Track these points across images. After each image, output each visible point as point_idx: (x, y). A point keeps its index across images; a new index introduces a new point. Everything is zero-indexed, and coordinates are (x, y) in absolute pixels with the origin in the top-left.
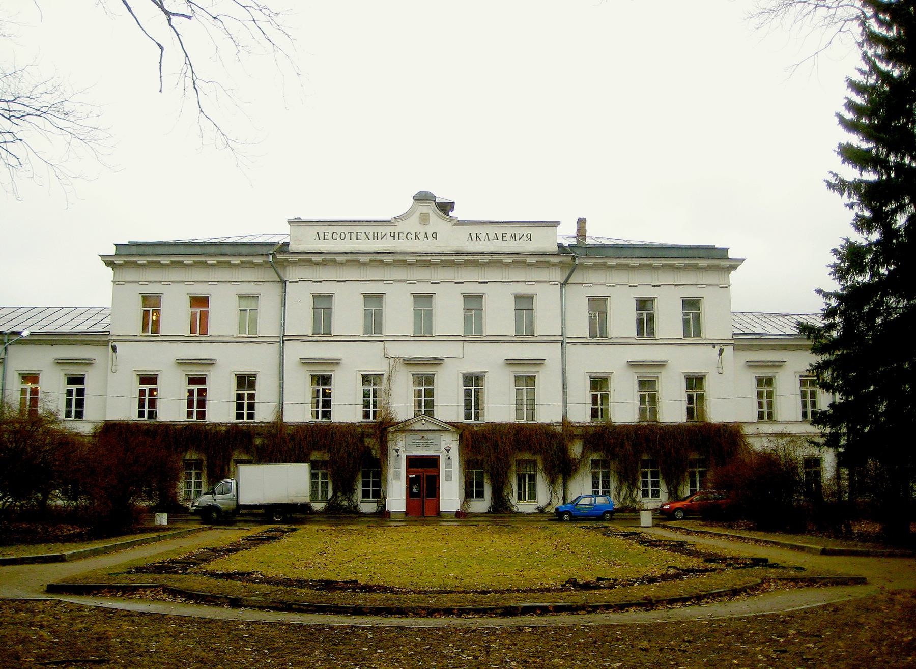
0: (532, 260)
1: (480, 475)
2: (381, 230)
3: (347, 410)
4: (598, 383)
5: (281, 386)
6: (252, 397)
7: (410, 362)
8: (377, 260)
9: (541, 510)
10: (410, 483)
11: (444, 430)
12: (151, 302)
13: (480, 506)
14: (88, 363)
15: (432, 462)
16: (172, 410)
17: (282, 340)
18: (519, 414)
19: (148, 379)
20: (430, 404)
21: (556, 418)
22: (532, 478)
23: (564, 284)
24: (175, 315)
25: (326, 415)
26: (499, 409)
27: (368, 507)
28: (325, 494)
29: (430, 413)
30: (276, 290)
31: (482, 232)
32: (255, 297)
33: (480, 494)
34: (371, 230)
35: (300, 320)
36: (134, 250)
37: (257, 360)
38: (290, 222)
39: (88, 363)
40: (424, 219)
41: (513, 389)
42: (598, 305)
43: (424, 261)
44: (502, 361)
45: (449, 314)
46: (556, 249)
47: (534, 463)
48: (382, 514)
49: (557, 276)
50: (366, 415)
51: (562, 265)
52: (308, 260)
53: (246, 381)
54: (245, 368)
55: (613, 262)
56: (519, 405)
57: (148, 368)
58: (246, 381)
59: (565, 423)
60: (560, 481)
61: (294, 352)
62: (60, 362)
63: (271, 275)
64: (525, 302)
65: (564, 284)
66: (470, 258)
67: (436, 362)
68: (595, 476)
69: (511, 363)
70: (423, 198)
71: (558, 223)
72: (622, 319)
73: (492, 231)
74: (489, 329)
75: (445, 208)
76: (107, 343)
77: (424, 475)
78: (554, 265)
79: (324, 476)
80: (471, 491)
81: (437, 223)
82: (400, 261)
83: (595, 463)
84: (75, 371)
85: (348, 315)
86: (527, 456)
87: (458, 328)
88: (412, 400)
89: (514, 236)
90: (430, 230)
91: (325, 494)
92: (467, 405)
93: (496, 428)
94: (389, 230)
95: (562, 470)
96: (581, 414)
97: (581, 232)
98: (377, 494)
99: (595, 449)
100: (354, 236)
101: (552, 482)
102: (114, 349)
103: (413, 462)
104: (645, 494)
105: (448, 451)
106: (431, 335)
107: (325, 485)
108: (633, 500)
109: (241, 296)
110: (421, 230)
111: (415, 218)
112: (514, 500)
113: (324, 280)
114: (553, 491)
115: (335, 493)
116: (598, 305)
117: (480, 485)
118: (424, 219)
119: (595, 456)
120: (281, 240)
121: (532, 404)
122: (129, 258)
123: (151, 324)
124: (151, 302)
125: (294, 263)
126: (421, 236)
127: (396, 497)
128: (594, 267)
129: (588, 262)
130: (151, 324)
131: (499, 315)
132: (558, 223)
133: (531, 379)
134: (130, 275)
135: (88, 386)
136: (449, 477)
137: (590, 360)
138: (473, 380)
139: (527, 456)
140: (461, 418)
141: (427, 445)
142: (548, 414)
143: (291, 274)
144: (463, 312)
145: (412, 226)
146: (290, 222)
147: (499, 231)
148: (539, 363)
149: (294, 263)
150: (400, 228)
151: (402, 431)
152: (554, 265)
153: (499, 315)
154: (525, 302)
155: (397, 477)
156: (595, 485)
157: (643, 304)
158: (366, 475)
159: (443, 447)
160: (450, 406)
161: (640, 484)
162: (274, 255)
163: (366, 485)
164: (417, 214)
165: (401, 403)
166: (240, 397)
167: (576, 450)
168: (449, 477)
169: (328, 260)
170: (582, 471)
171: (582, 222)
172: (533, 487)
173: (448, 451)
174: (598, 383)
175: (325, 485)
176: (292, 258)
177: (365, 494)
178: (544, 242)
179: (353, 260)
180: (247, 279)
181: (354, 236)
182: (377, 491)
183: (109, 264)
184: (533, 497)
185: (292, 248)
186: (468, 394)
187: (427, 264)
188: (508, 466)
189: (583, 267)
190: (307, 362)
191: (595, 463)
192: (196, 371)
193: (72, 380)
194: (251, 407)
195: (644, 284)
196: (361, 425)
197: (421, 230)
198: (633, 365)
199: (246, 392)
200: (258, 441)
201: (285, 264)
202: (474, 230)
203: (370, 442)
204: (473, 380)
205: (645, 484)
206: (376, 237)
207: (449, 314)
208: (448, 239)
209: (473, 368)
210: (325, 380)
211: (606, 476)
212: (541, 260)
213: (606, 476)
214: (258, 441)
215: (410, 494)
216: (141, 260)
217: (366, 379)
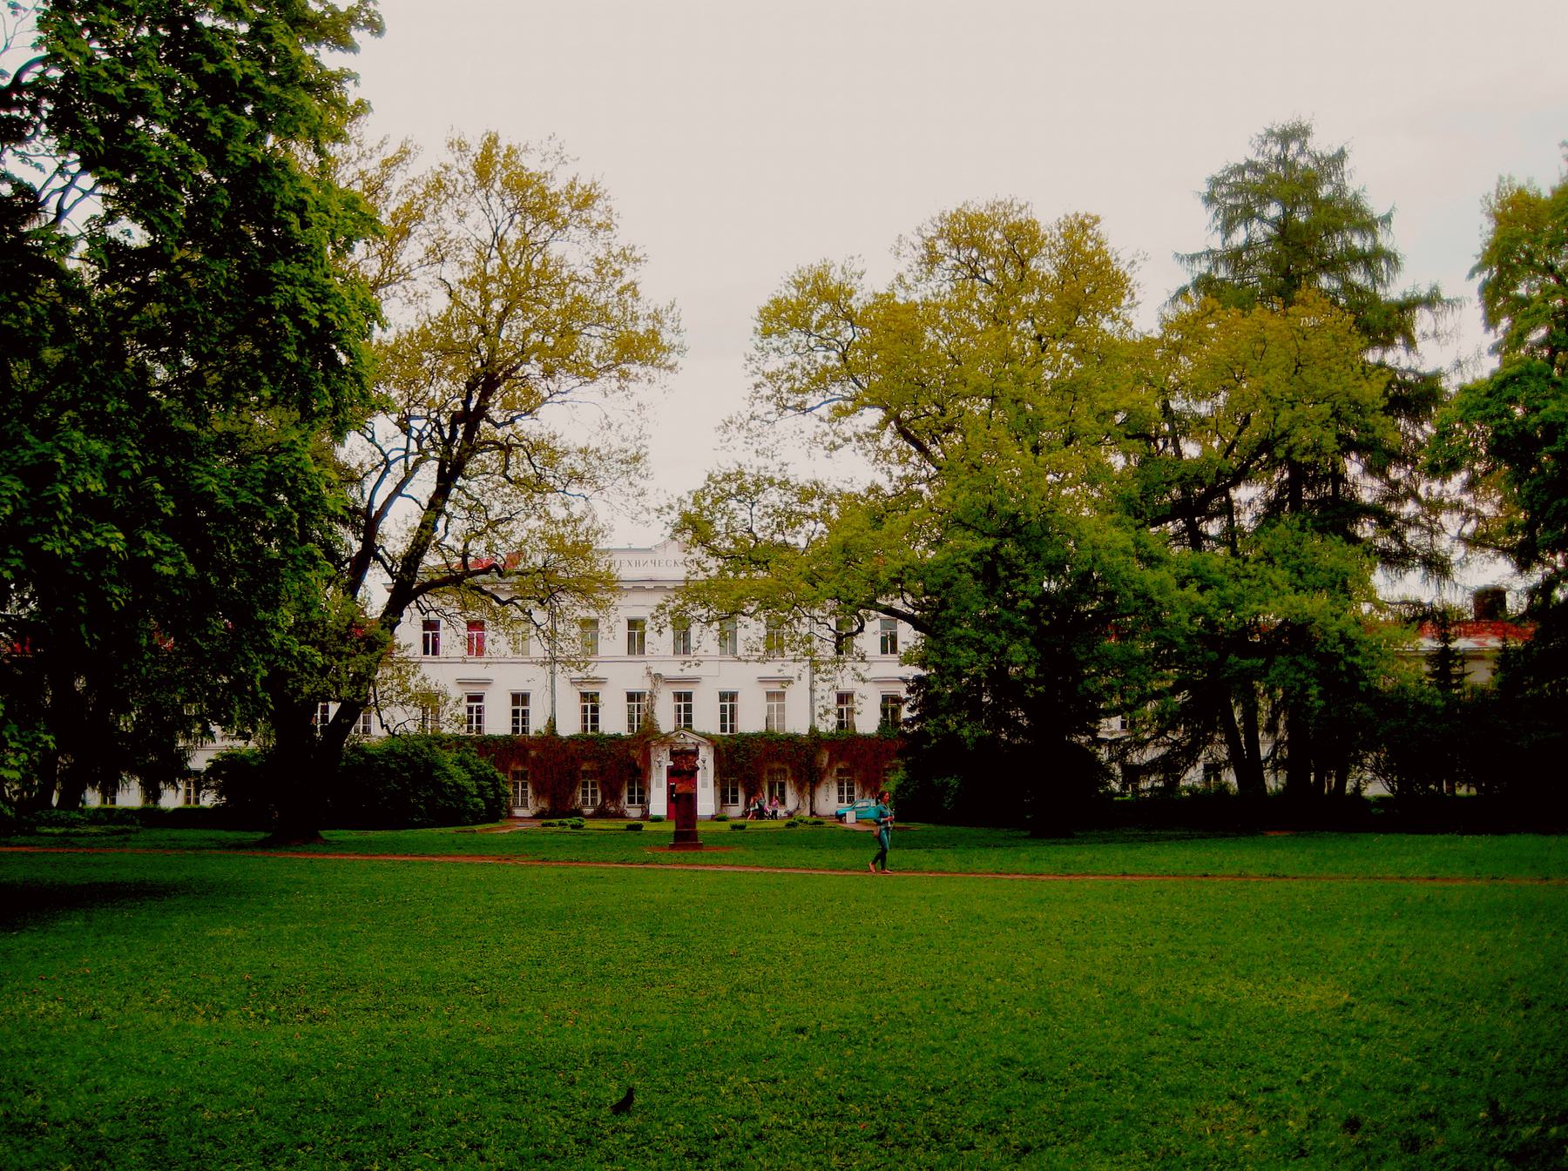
1: (735, 784)
2: (643, 557)
3: (614, 721)
5: (553, 703)
6: (525, 713)
10: (671, 790)
13: (736, 810)
20: (688, 719)
21: (804, 730)
22: (782, 786)
27: (634, 812)
29: (689, 727)
33: (735, 800)
47: (784, 771)
53: (520, 699)
54: (520, 688)
58: (520, 699)
60: (807, 789)
68: (840, 784)
79: (593, 785)
80: (725, 798)
83: (840, 772)
86: (776, 766)
88: (672, 713)
92: (723, 719)
93: (748, 738)
94: (649, 557)
95: (809, 779)
96: (827, 726)
98: (641, 800)
99: (841, 758)
101: (800, 790)
107: (594, 793)
117: (735, 792)
119: (841, 766)
135: (485, 703)
136: (705, 785)
142: (797, 723)
150: (660, 555)
156: (841, 791)
158: (631, 783)
160: (707, 720)
163: (631, 792)
165: (666, 720)
166: (515, 713)
167: (825, 758)
168: (705, 785)
170: (828, 779)
172: (782, 793)
175: (594, 793)
177: (631, 801)
184: (783, 802)
186: (723, 709)
188: (760, 775)
192: (475, 690)
199: (521, 708)
200: (533, 753)
203: (634, 753)
204: (728, 697)
206: (637, 564)
209: (728, 688)
211: (851, 784)
213: (851, 784)
214: (533, 753)
215: (671, 800)
217: (631, 697)
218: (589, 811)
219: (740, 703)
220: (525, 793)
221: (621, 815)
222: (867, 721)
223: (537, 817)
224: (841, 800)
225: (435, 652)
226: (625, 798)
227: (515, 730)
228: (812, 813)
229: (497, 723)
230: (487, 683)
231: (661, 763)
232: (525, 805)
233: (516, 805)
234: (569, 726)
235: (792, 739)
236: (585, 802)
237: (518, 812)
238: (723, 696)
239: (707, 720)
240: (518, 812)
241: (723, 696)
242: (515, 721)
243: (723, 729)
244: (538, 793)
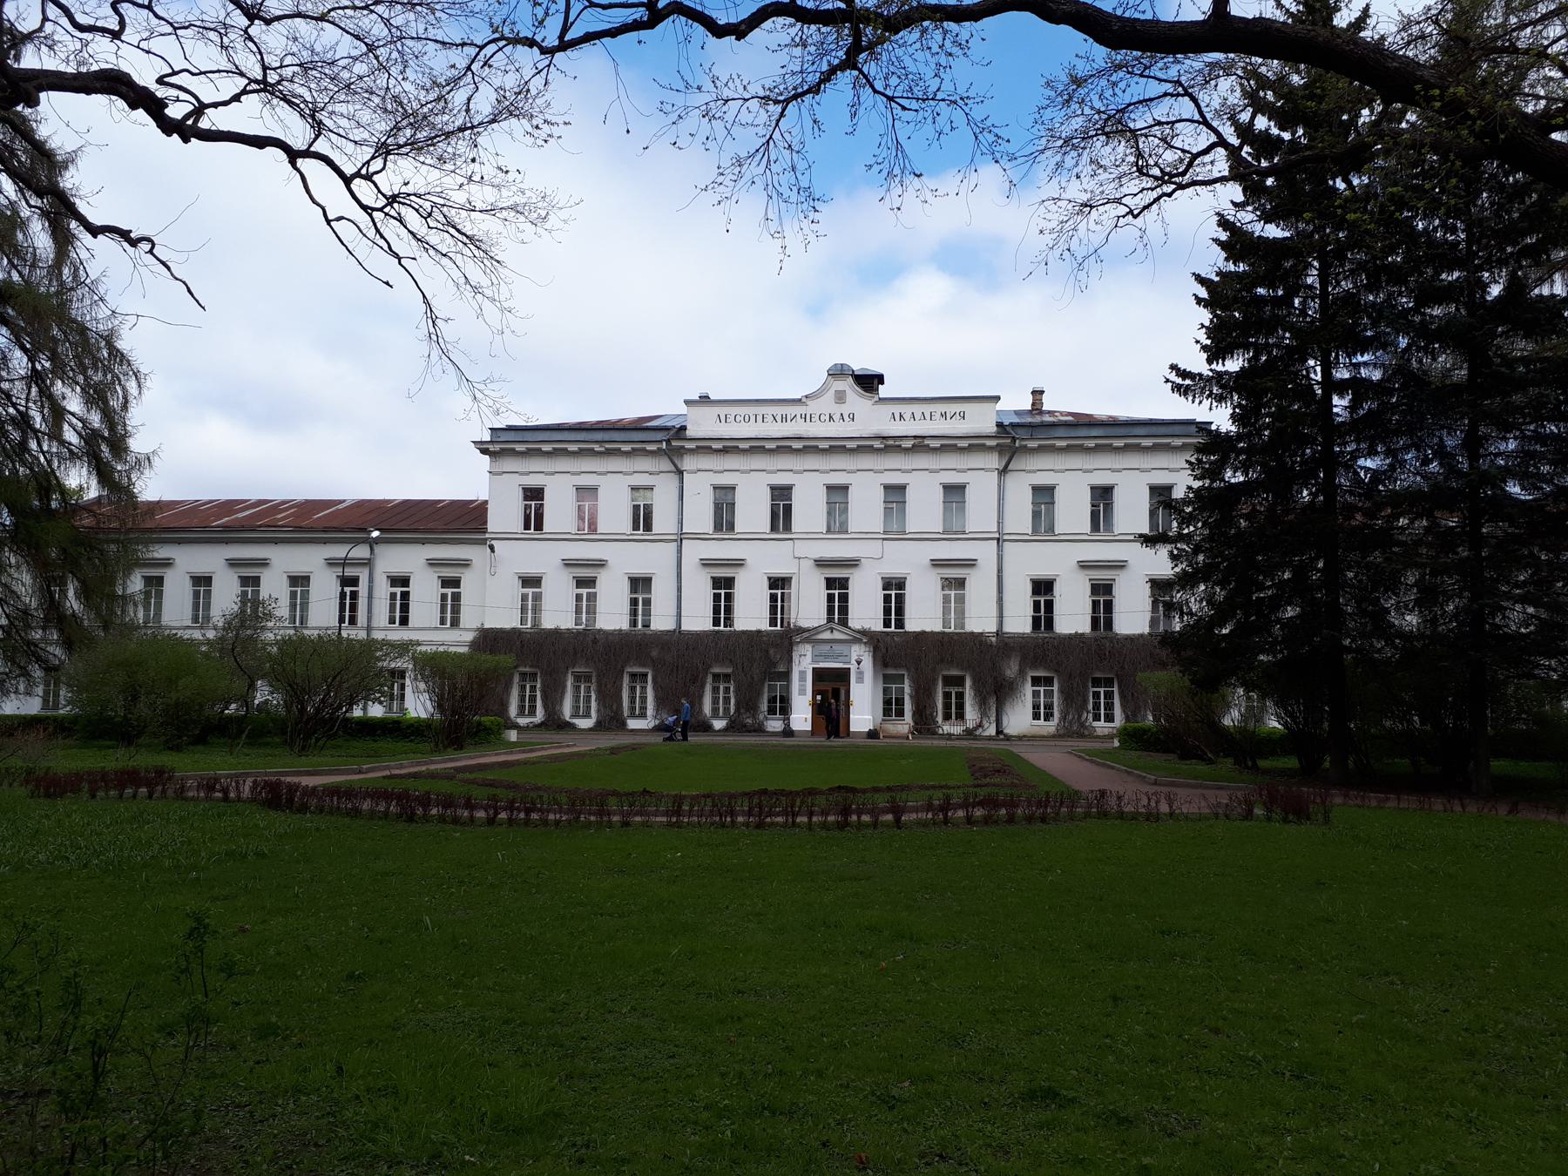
0: (964, 443)
3: (751, 614)
4: (1043, 587)
5: (679, 589)
6: (647, 602)
7: (821, 563)
8: (783, 447)
9: (969, 733)
11: (855, 641)
12: (534, 494)
14: (465, 564)
15: (842, 676)
16: (558, 614)
17: (680, 538)
18: (946, 623)
19: (531, 581)
20: (844, 610)
21: (991, 627)
22: (960, 696)
23: (1003, 471)
24: (559, 511)
25: (729, 621)
26: (923, 615)
27: (775, 725)
28: (727, 710)
29: (844, 622)
30: (673, 480)
31: (907, 410)
32: (651, 488)
33: (900, 713)
34: (778, 410)
35: (700, 516)
36: (511, 436)
37: (652, 559)
38: (687, 402)
39: (465, 564)
40: (840, 397)
41: (940, 595)
42: (1044, 495)
43: (837, 447)
44: (927, 562)
45: (866, 507)
46: (992, 429)
48: (788, 732)
49: (993, 461)
50: (773, 622)
51: (1000, 449)
52: (706, 447)
53: (640, 584)
54: (640, 570)
55: (1063, 443)
56: (946, 611)
57: (532, 570)
59: (999, 633)
61: (694, 552)
62: (433, 563)
63: (665, 465)
64: (954, 492)
65: (1003, 471)
66: (891, 442)
67: (852, 563)
69: (937, 564)
70: (838, 372)
71: (998, 398)
72: (1073, 510)
73: (918, 409)
74: (912, 526)
75: (869, 382)
76: (483, 542)
77: (832, 691)
78: (991, 448)
81: (857, 401)
82: (810, 447)
84: (449, 573)
85: (753, 511)
87: (876, 523)
89: (944, 415)
90: (845, 409)
91: (727, 710)
92: (887, 611)
96: (1020, 622)
97: (1037, 407)
100: (760, 418)
101: (982, 703)
102: (492, 548)
103: (819, 675)
104: (1097, 718)
105: (859, 663)
106: (846, 532)
108: (1082, 725)
109: (634, 489)
110: (836, 410)
111: (831, 394)
112: (940, 719)
113: (728, 470)
114: (984, 714)
115: (737, 709)
116: (1044, 495)
118: (840, 397)
120: (677, 423)
121: (961, 613)
122: (504, 445)
123: (534, 520)
124: (534, 494)
125: (691, 451)
126: (837, 417)
127: (802, 717)
128: (1041, 449)
129: (1033, 444)
130: (534, 520)
131: (925, 507)
132: (998, 398)
133: (960, 583)
134: (509, 464)
137: (1029, 562)
138: (894, 587)
139: (955, 672)
140: (878, 626)
141: (835, 657)
142: (980, 620)
143: (688, 463)
144: (882, 505)
145: (826, 405)
146: (687, 402)
147: (927, 409)
148: (970, 564)
149: (691, 451)
150: (813, 407)
151: (807, 640)
152: (991, 448)
153: (925, 507)
154: (954, 492)
155: (802, 692)
157: (1103, 496)
159: (854, 657)
160: (866, 611)
161: (1090, 707)
162: (668, 441)
164: (831, 393)
166: (634, 602)
169: (729, 448)
171: (1037, 394)
172: (961, 707)
173: (859, 663)
174: (1043, 587)
176: (692, 445)
177: (772, 711)
178: (982, 422)
179: (757, 447)
180: (643, 470)
181: (760, 418)
182: (782, 706)
183: (484, 451)
184: (961, 716)
185: (690, 433)
187: (842, 450)
189: (1026, 450)
190: (707, 563)
191: (1036, 681)
192: (585, 573)
193: (447, 583)
194: (647, 613)
195: (1102, 469)
196: (768, 633)
197: (836, 410)
198: (1084, 566)
201: (681, 452)
202: (897, 409)
205: (1097, 706)
206: (784, 419)
207: (866, 507)
208: (868, 418)
209: (894, 571)
210: (728, 583)
212: (974, 445)
216: (520, 448)
218: (719, 724)
219: (910, 593)
220: (644, 699)
221: (759, 729)
222: (1072, 617)
223: (657, 729)
224: (1036, 716)
225: (539, 527)
226: (764, 706)
227: (634, 623)
228: (999, 732)
229: (612, 616)
230: (600, 564)
231: (804, 663)
232: (643, 715)
233: (633, 715)
234: (699, 619)
235: (977, 638)
236: (715, 710)
237: (633, 724)
238: (888, 584)
239: (866, 611)
240: (633, 724)
241: (888, 584)
242: (634, 613)
243: (887, 624)
244: (661, 702)
